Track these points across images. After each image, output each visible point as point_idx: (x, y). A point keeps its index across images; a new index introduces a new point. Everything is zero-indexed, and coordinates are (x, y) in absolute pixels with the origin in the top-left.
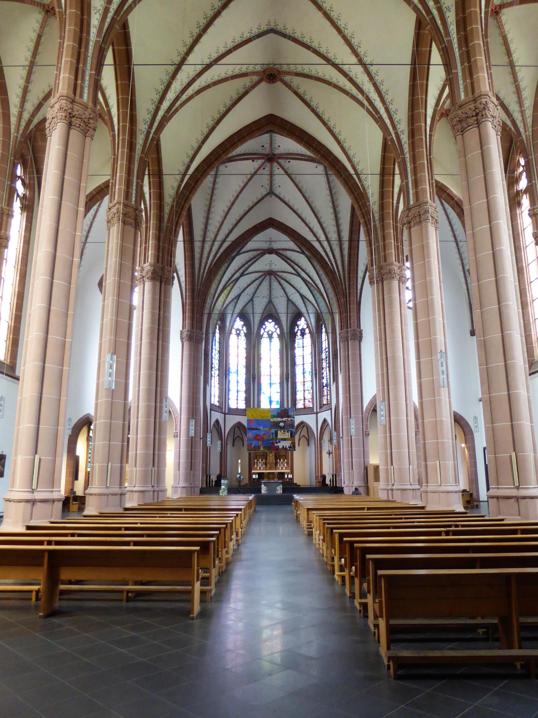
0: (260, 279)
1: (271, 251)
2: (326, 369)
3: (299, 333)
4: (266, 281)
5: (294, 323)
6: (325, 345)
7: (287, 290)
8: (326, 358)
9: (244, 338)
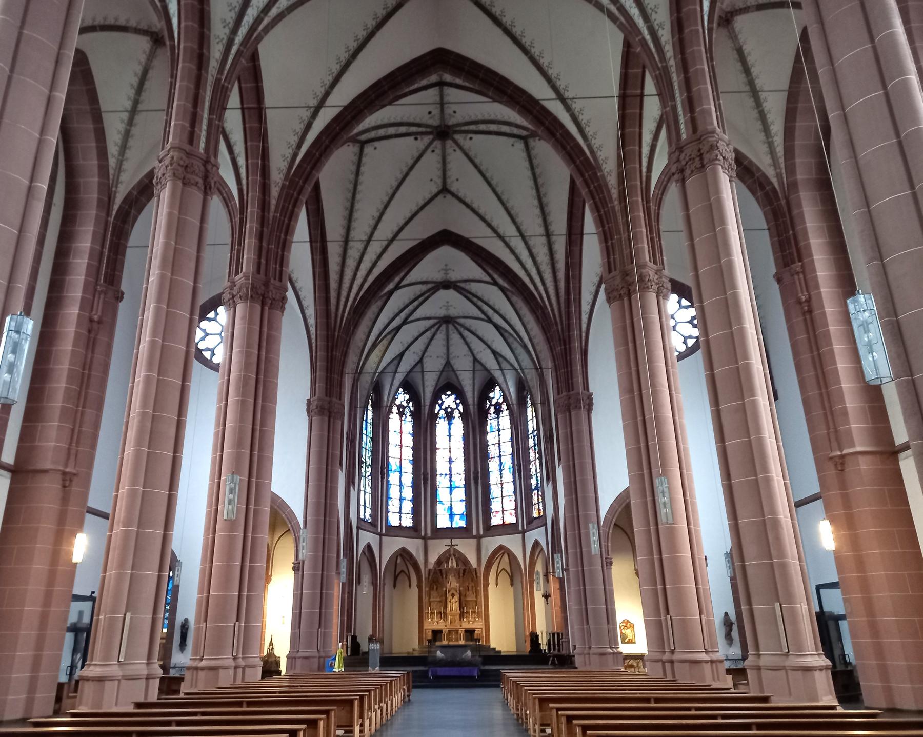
0: (433, 330)
1: (447, 285)
2: (535, 463)
3: (492, 410)
4: (441, 333)
5: (484, 396)
6: (532, 425)
7: (473, 346)
8: (535, 446)
9: (409, 419)
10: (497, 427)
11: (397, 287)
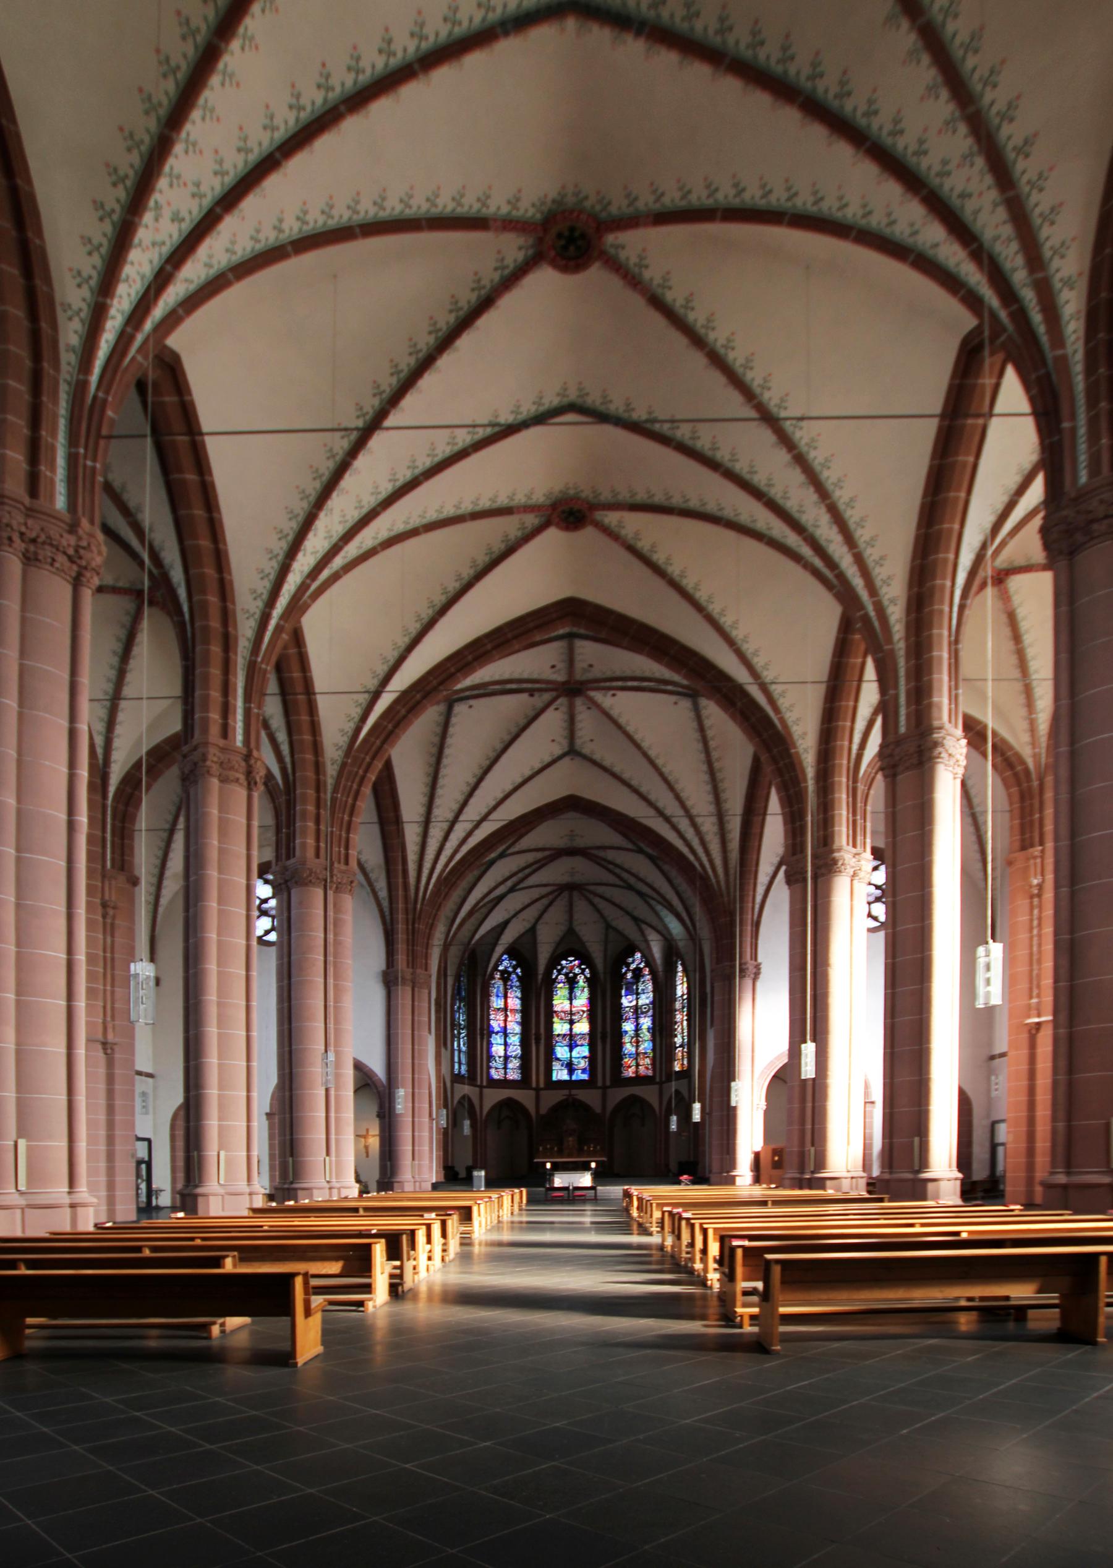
0: (551, 897)
11: (502, 856)
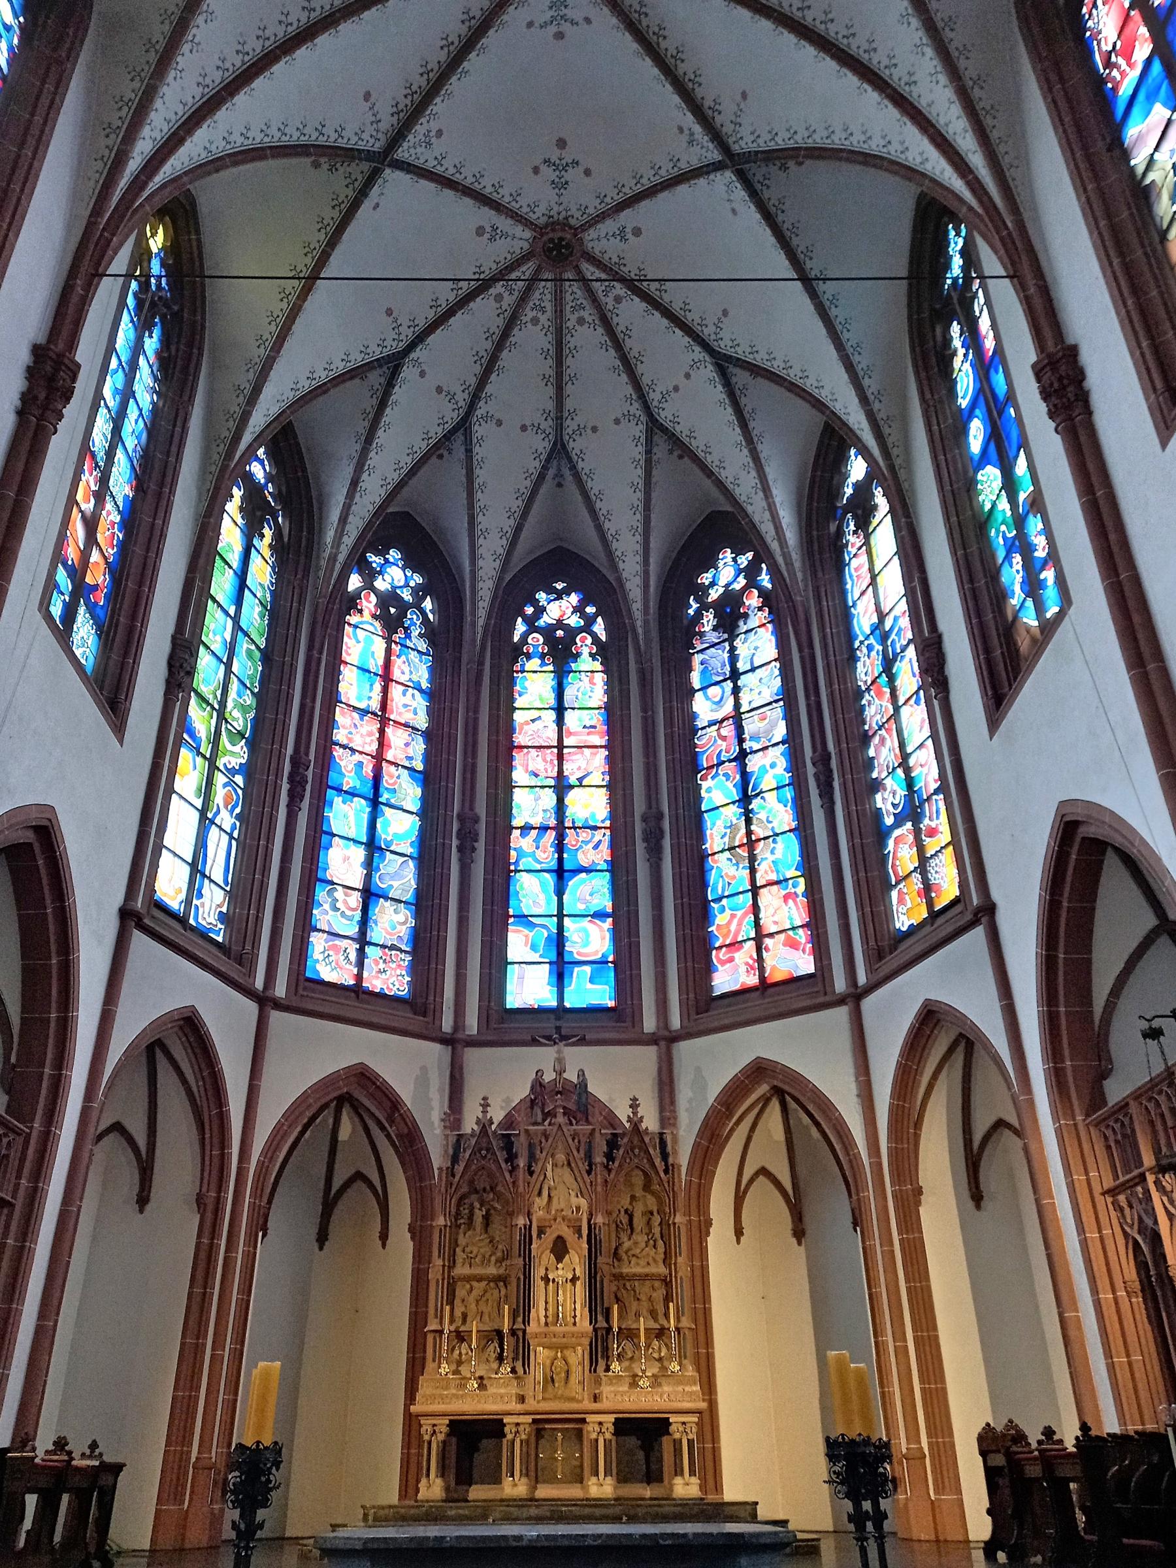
3: (709, 620)
10: (728, 669)
